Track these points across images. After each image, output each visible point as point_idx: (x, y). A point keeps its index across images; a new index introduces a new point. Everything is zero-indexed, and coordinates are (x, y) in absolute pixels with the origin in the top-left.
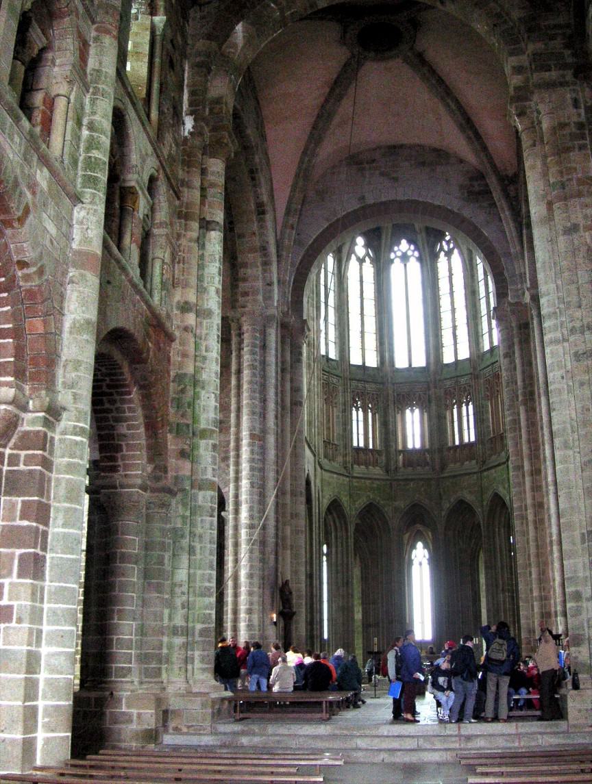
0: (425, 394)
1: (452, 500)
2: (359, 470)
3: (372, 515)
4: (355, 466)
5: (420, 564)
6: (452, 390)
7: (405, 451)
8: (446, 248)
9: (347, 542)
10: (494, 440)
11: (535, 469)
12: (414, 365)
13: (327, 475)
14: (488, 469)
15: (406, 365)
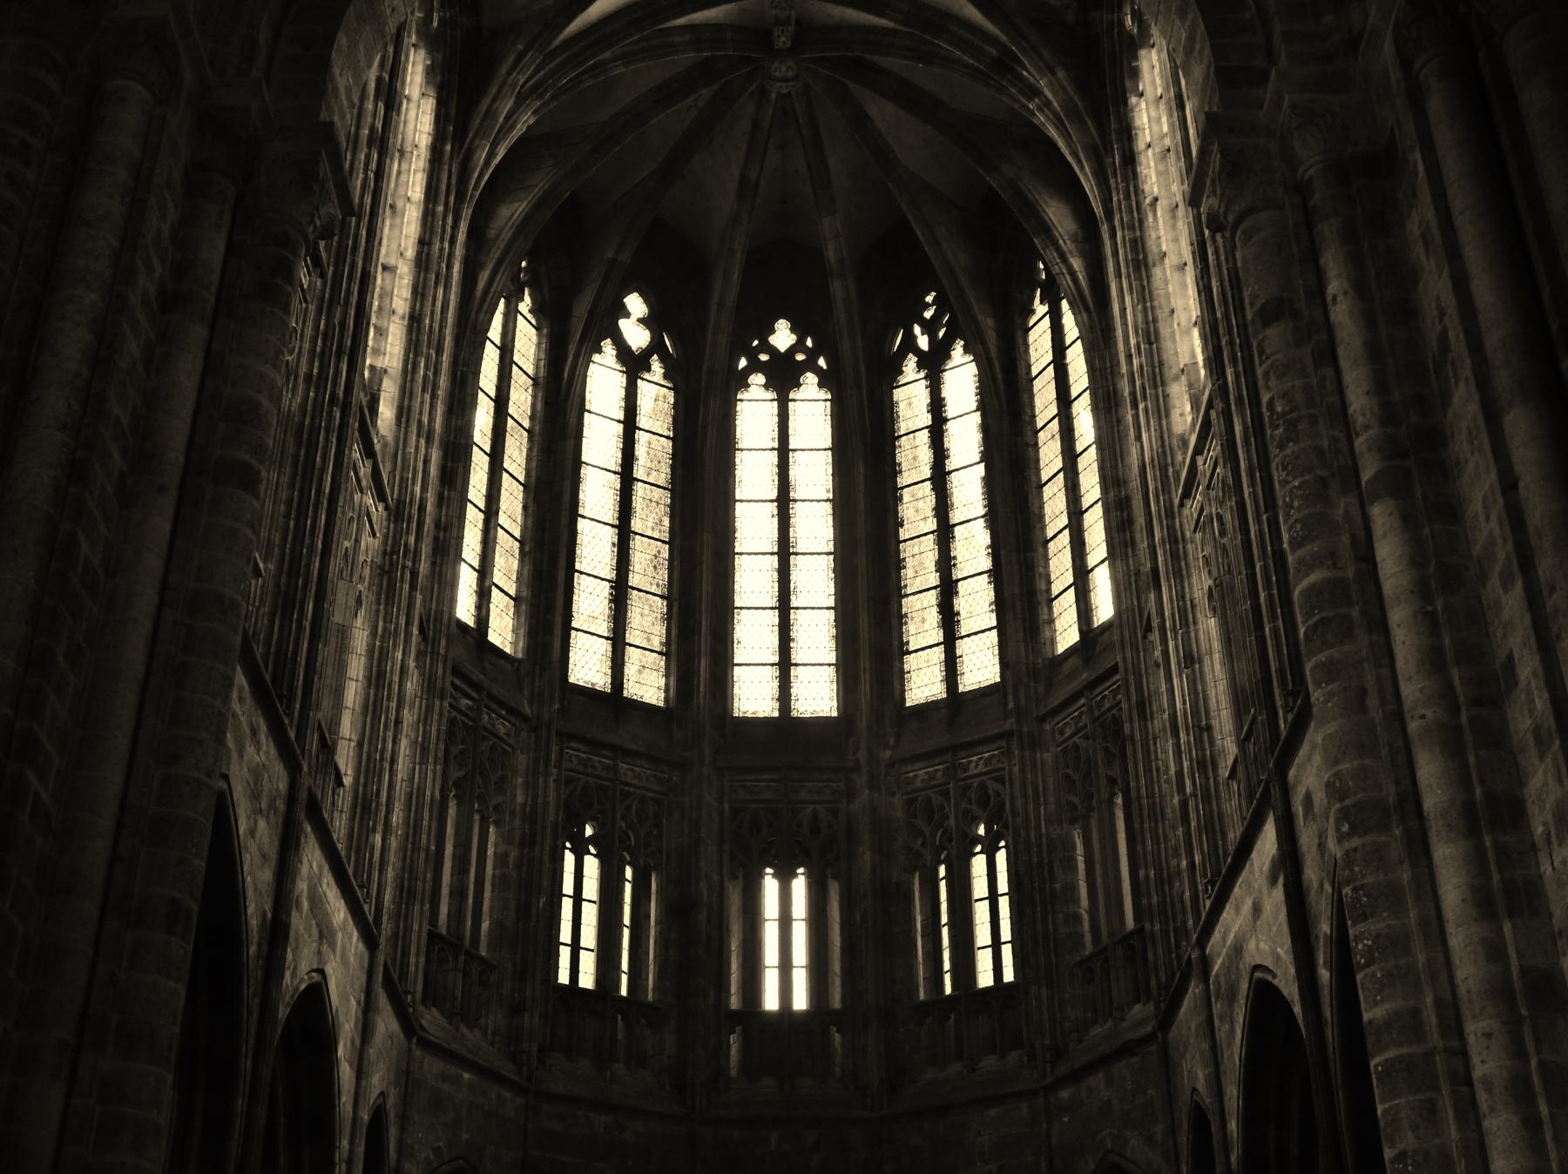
8: (923, 342)
12: (794, 714)
13: (433, 1066)
14: (1077, 1076)
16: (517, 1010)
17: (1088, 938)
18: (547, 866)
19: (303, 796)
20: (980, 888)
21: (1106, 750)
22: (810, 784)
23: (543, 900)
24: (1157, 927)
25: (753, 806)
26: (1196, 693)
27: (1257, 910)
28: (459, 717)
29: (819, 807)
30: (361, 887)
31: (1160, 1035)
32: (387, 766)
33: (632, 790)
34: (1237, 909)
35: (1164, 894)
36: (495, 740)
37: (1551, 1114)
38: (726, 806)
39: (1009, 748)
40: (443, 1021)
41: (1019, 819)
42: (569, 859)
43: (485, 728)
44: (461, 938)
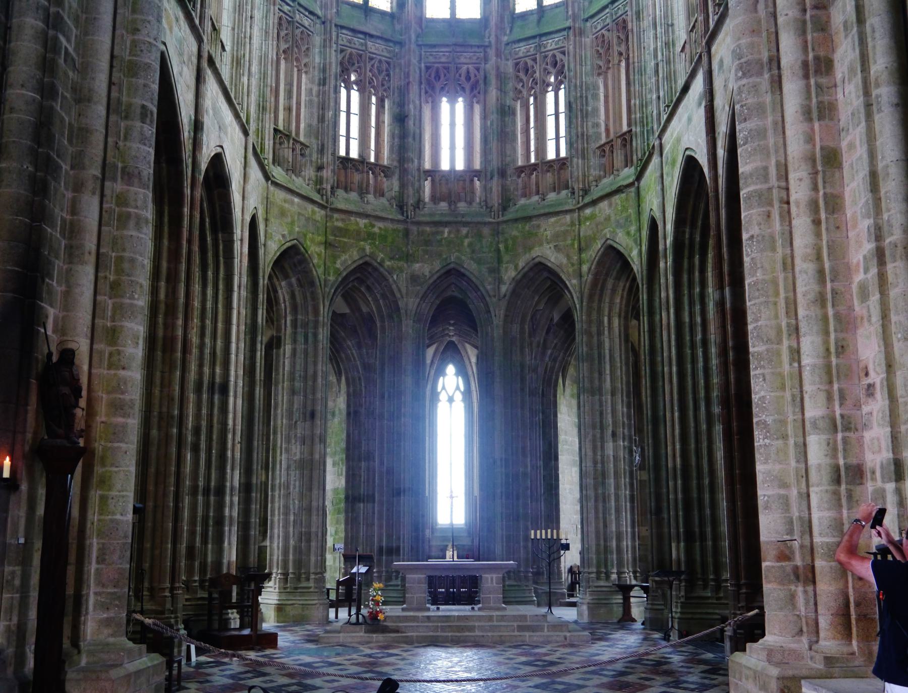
0: (478, 69)
1: (521, 264)
2: (344, 200)
3: (369, 288)
4: (340, 193)
5: (451, 400)
6: (530, 63)
7: (434, 173)
9: (315, 335)
10: (607, 148)
11: (817, 58)
12: (457, 16)
13: (279, 196)
14: (594, 203)
15: (446, 14)
16: (320, 168)
17: (604, 135)
18: (332, 95)
19: (205, 55)
20: (550, 109)
21: (619, 37)
22: (465, 54)
23: (331, 113)
24: (638, 129)
25: (436, 65)
26: (667, 6)
27: (690, 120)
28: (284, 15)
29: (470, 66)
30: (238, 104)
31: (636, 183)
32: (248, 40)
33: (374, 56)
34: (680, 120)
35: (643, 113)
36: (303, 28)
37: (827, 218)
38: (423, 65)
39: (568, 35)
40: (284, 173)
41: (572, 74)
42: (343, 92)
43: (297, 22)
44: (291, 132)
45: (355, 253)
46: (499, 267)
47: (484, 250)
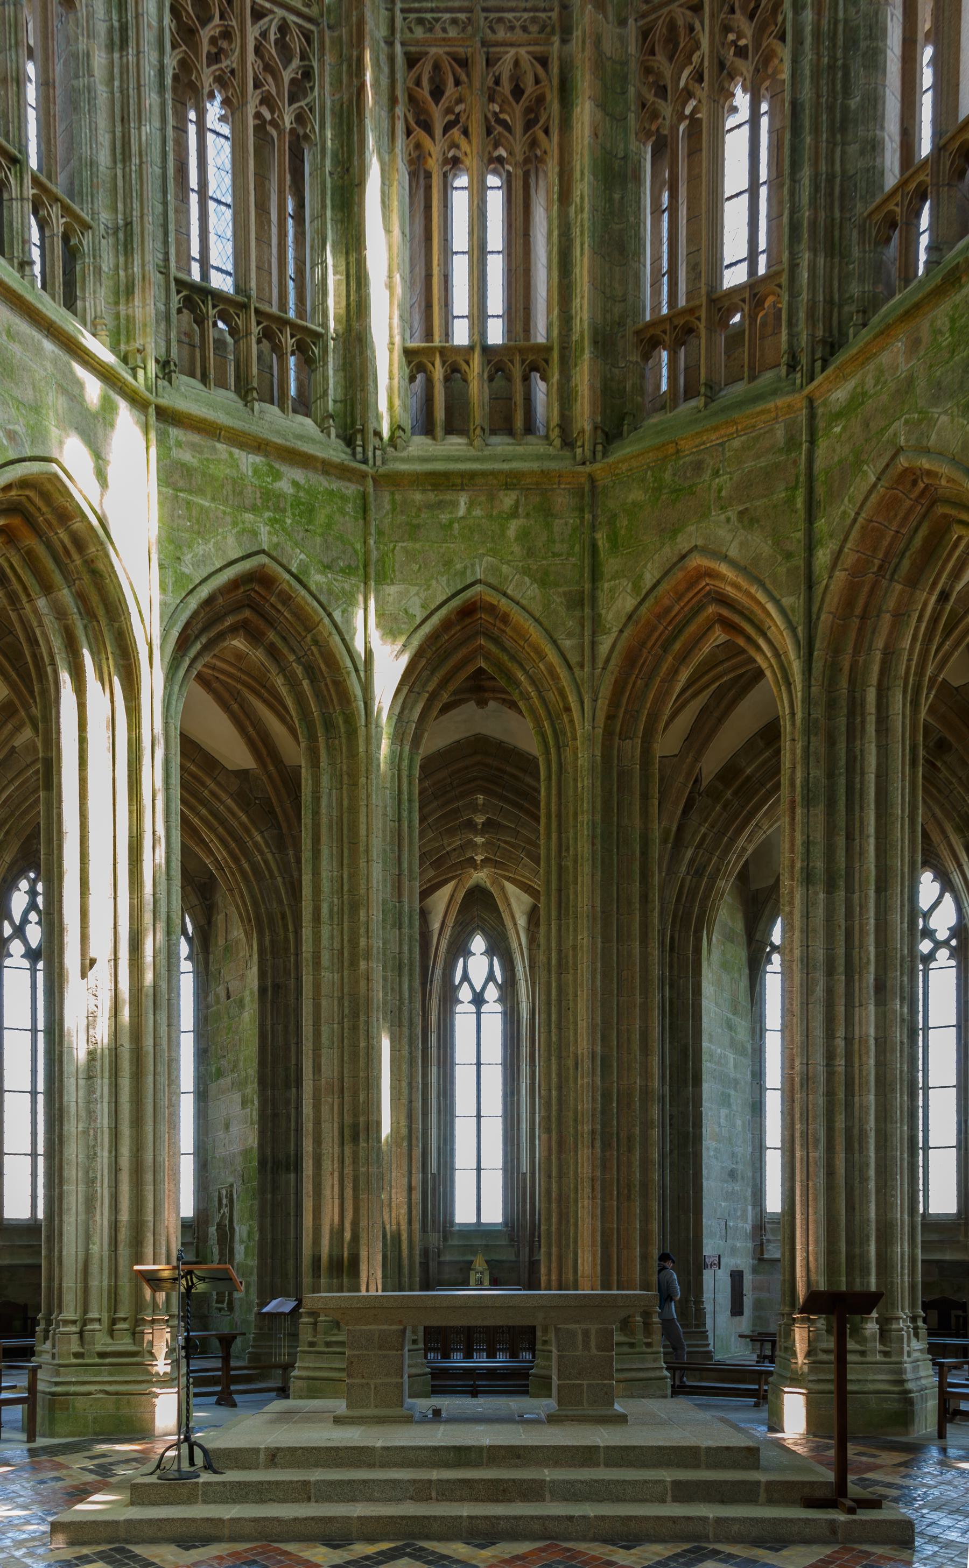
45: (231, 540)
46: (594, 589)
47: (558, 547)
